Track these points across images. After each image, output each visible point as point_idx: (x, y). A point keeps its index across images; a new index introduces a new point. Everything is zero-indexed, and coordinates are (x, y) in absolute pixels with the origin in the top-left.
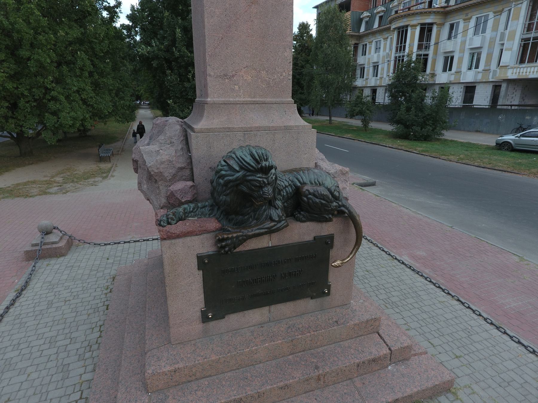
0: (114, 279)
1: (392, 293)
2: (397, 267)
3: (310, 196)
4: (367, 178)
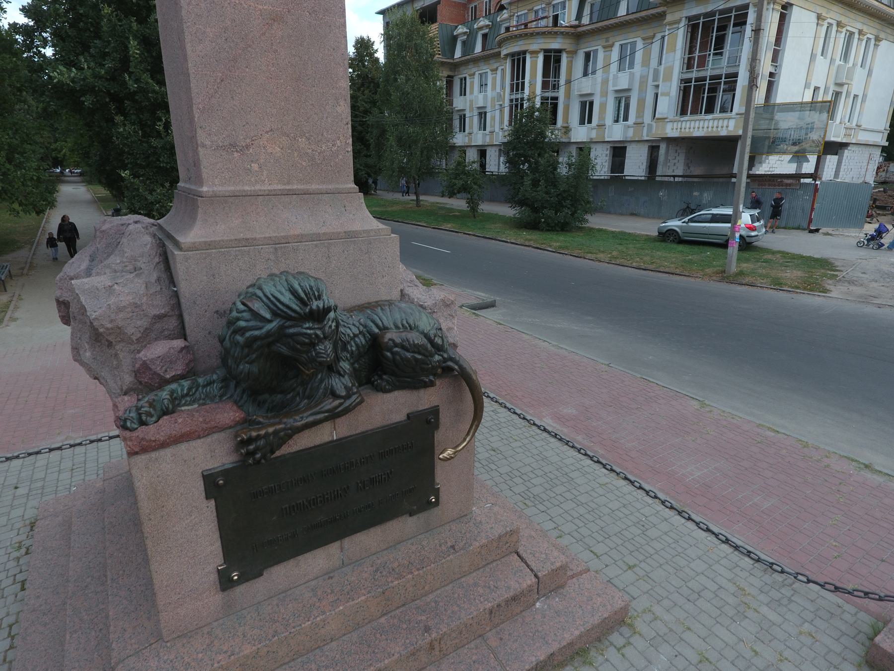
0: (32, 526)
1: (533, 481)
2: (536, 437)
3: (396, 349)
4: (483, 296)
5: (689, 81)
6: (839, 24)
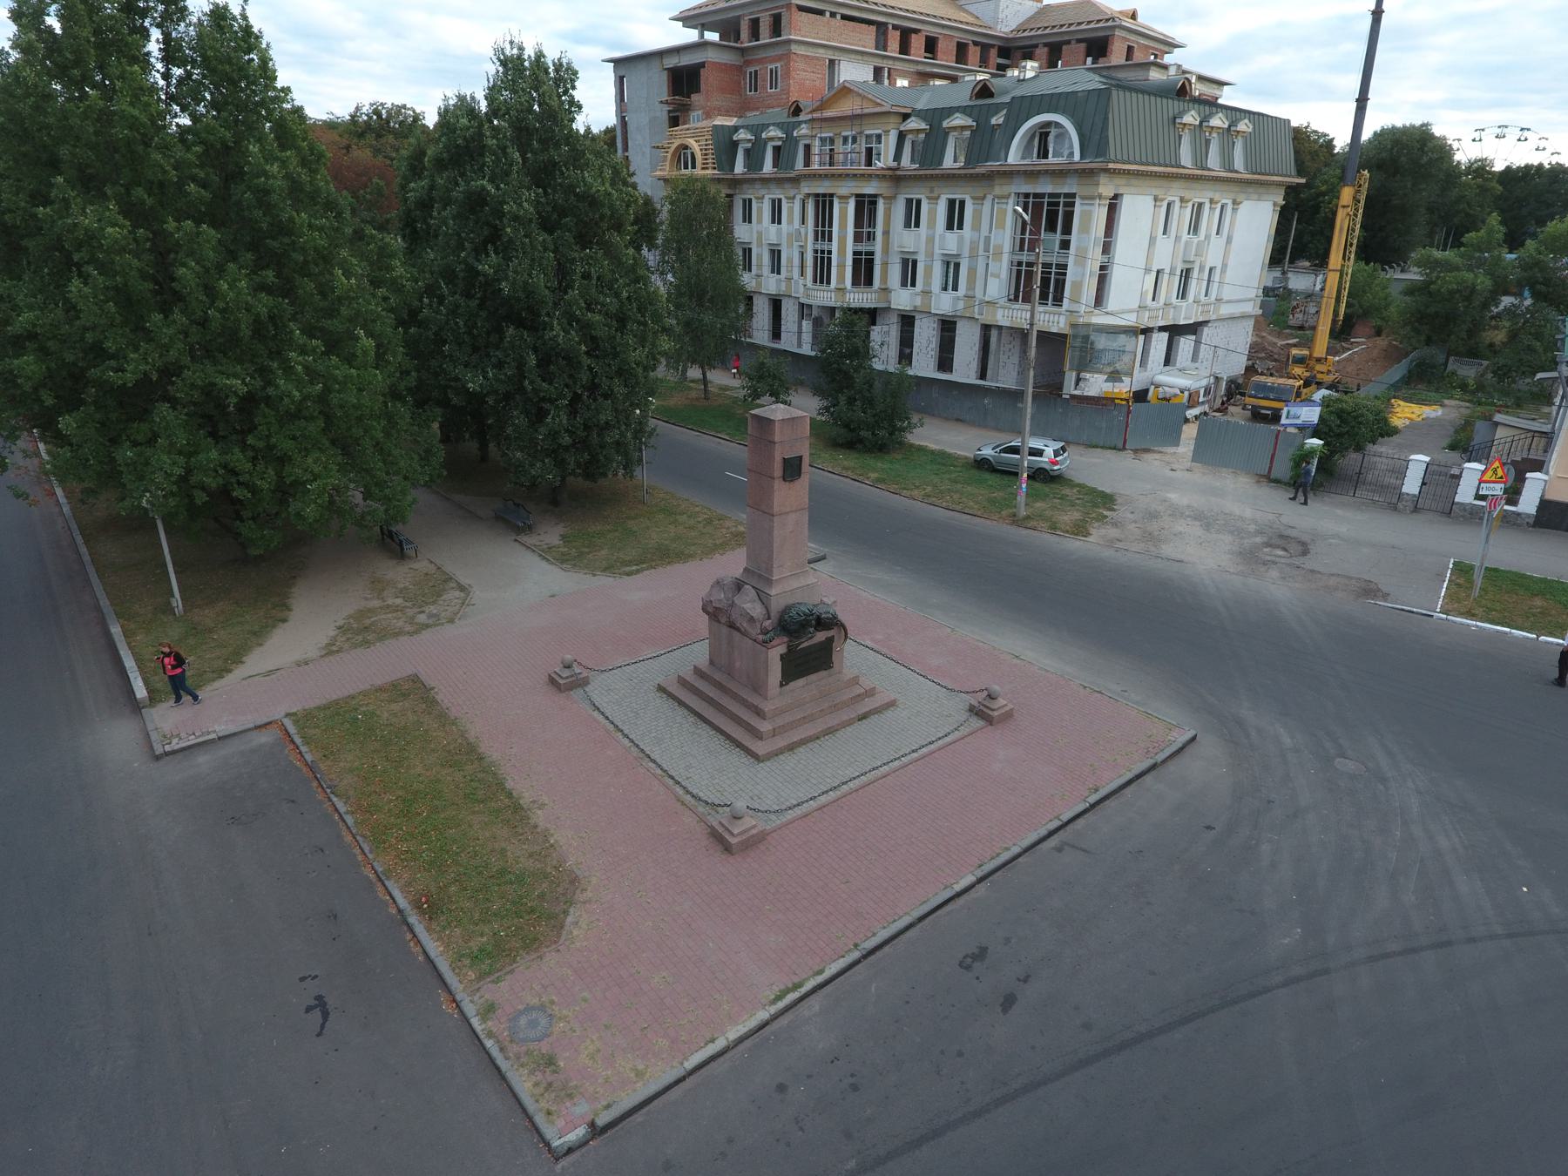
5: (1020, 264)
6: (1182, 200)
